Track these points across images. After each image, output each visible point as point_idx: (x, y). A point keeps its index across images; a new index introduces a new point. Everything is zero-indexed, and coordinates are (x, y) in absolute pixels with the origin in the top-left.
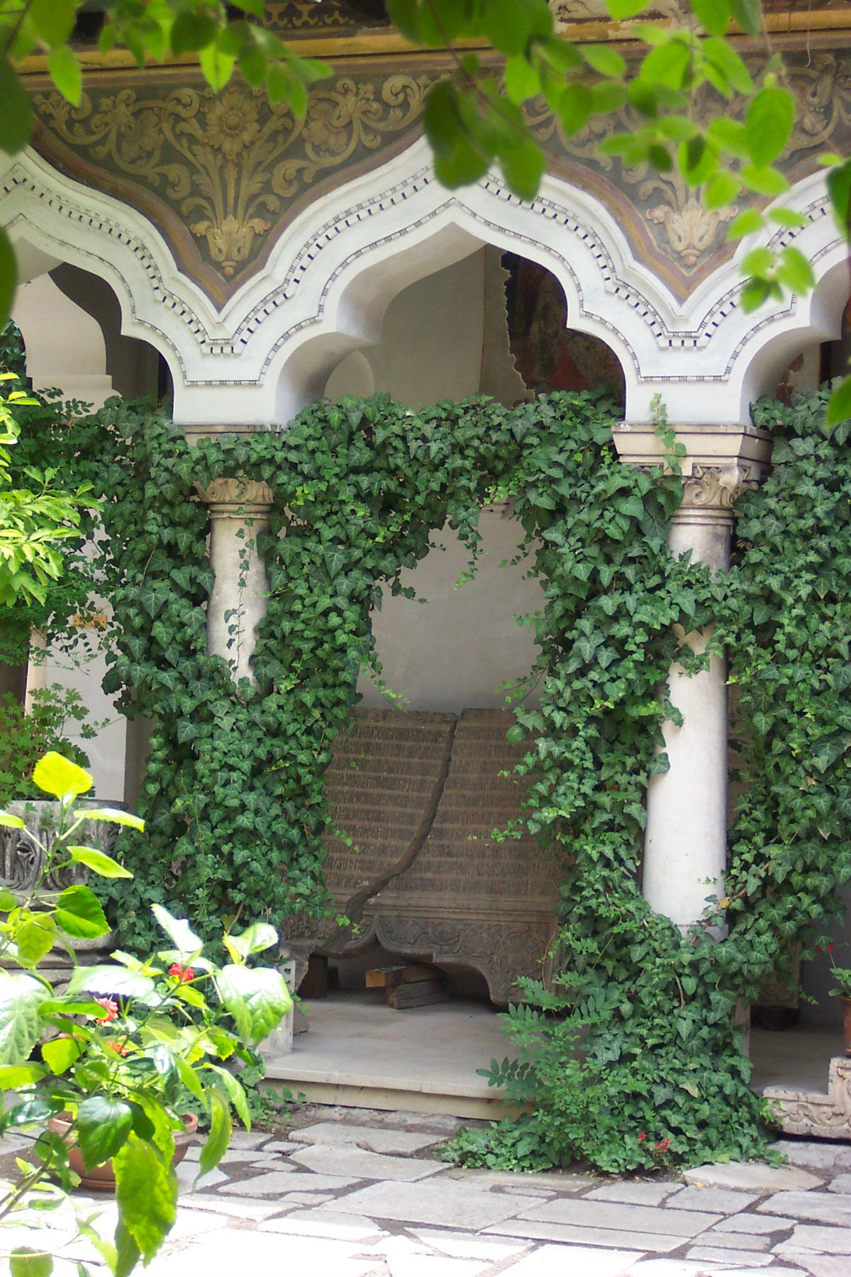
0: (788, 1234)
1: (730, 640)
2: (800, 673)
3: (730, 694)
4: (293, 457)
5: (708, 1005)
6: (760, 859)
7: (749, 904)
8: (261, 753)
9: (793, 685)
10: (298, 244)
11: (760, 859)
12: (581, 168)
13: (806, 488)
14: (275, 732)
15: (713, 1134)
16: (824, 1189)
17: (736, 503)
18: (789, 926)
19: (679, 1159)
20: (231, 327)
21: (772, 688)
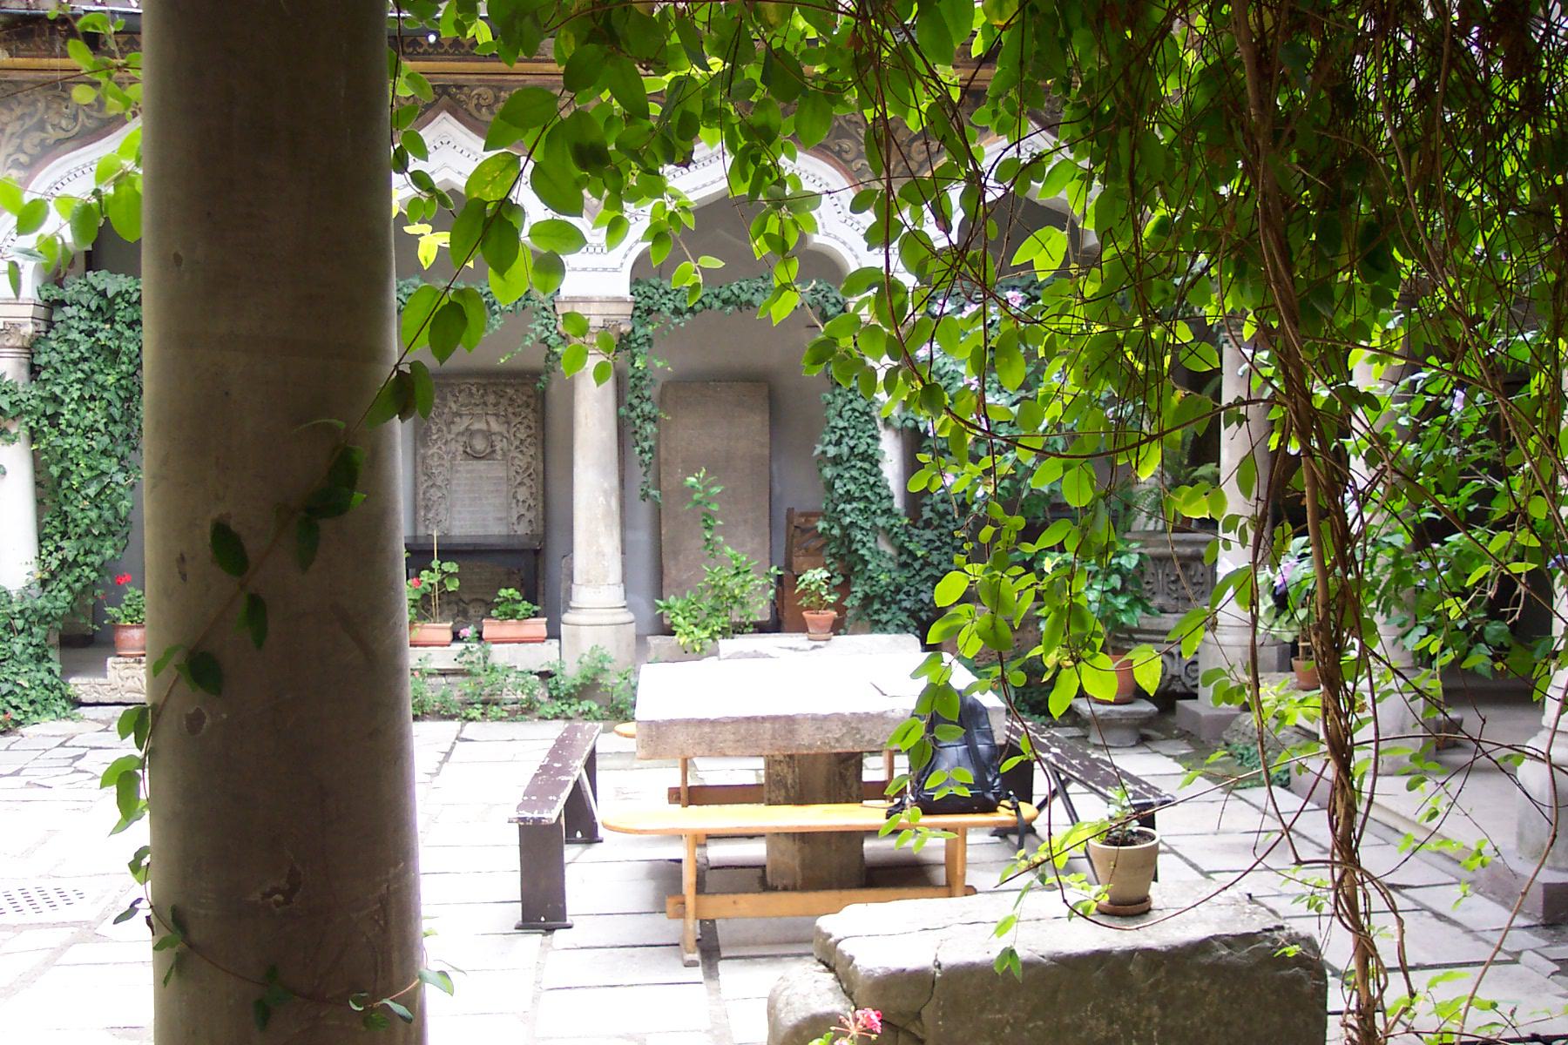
0: (83, 756)
1: (33, 424)
2: (76, 441)
3: (35, 455)
5: (31, 635)
6: (58, 549)
7: (53, 574)
9: (72, 448)
11: (58, 549)
13: (74, 335)
15: (39, 707)
16: (106, 730)
17: (32, 345)
18: (78, 586)
19: (19, 723)
21: (59, 451)
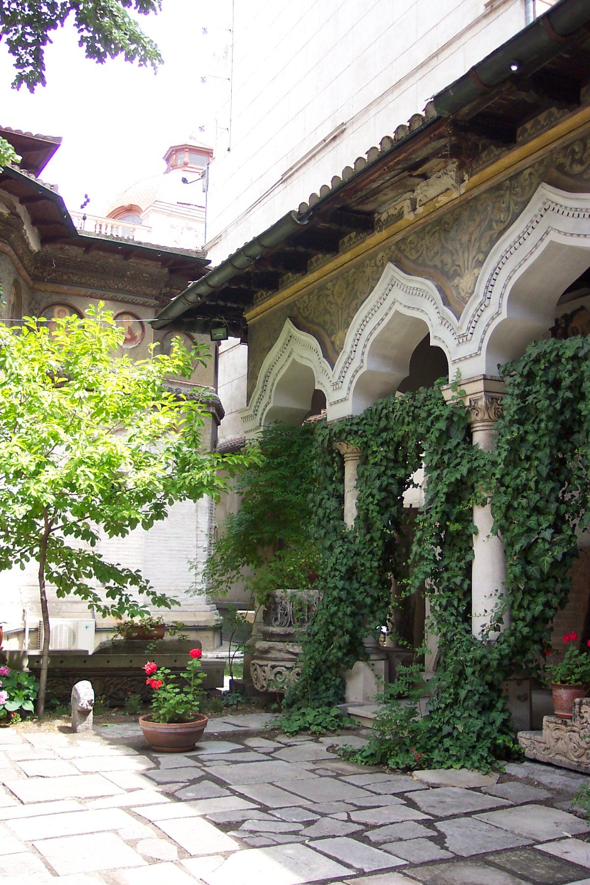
4: (355, 428)
8: (350, 563)
10: (353, 335)
12: (432, 270)
14: (357, 554)
20: (337, 376)
